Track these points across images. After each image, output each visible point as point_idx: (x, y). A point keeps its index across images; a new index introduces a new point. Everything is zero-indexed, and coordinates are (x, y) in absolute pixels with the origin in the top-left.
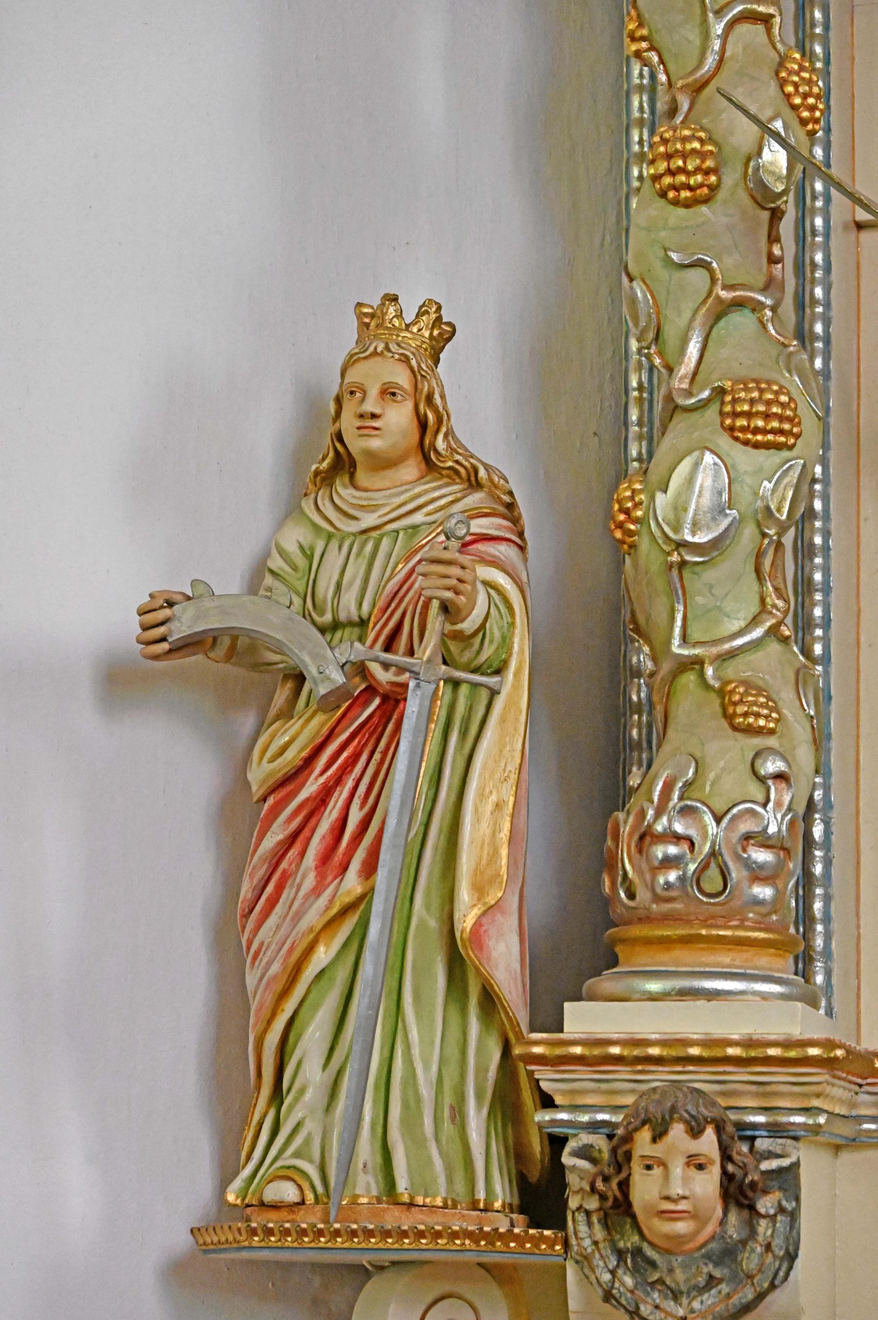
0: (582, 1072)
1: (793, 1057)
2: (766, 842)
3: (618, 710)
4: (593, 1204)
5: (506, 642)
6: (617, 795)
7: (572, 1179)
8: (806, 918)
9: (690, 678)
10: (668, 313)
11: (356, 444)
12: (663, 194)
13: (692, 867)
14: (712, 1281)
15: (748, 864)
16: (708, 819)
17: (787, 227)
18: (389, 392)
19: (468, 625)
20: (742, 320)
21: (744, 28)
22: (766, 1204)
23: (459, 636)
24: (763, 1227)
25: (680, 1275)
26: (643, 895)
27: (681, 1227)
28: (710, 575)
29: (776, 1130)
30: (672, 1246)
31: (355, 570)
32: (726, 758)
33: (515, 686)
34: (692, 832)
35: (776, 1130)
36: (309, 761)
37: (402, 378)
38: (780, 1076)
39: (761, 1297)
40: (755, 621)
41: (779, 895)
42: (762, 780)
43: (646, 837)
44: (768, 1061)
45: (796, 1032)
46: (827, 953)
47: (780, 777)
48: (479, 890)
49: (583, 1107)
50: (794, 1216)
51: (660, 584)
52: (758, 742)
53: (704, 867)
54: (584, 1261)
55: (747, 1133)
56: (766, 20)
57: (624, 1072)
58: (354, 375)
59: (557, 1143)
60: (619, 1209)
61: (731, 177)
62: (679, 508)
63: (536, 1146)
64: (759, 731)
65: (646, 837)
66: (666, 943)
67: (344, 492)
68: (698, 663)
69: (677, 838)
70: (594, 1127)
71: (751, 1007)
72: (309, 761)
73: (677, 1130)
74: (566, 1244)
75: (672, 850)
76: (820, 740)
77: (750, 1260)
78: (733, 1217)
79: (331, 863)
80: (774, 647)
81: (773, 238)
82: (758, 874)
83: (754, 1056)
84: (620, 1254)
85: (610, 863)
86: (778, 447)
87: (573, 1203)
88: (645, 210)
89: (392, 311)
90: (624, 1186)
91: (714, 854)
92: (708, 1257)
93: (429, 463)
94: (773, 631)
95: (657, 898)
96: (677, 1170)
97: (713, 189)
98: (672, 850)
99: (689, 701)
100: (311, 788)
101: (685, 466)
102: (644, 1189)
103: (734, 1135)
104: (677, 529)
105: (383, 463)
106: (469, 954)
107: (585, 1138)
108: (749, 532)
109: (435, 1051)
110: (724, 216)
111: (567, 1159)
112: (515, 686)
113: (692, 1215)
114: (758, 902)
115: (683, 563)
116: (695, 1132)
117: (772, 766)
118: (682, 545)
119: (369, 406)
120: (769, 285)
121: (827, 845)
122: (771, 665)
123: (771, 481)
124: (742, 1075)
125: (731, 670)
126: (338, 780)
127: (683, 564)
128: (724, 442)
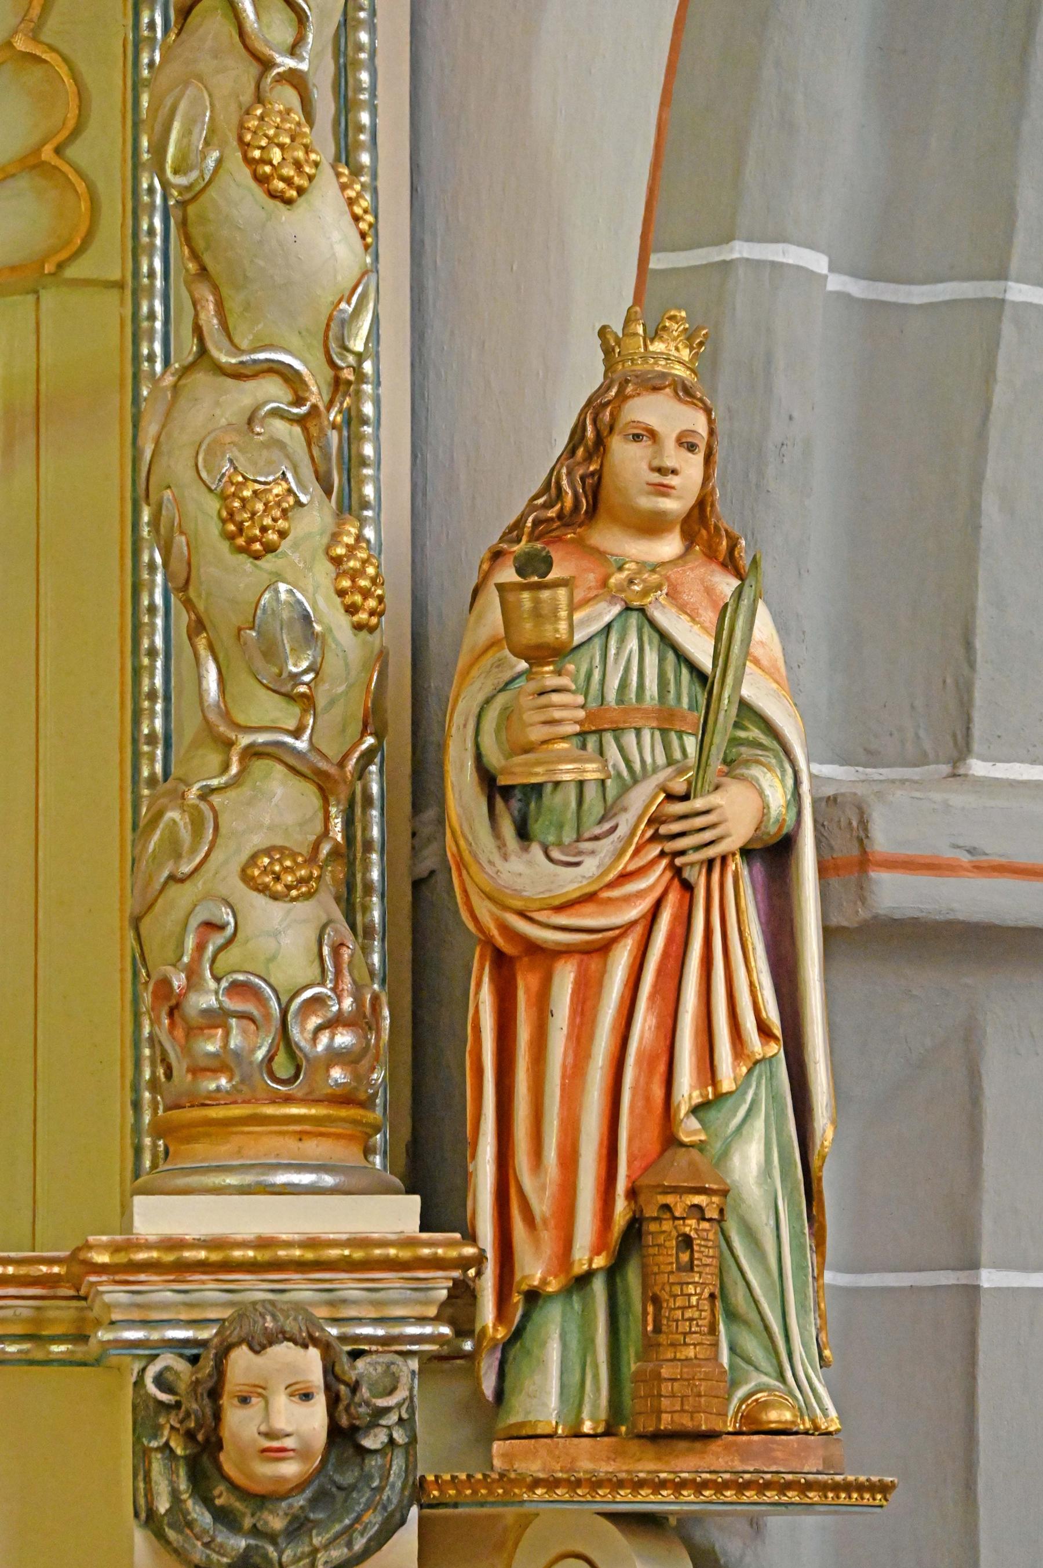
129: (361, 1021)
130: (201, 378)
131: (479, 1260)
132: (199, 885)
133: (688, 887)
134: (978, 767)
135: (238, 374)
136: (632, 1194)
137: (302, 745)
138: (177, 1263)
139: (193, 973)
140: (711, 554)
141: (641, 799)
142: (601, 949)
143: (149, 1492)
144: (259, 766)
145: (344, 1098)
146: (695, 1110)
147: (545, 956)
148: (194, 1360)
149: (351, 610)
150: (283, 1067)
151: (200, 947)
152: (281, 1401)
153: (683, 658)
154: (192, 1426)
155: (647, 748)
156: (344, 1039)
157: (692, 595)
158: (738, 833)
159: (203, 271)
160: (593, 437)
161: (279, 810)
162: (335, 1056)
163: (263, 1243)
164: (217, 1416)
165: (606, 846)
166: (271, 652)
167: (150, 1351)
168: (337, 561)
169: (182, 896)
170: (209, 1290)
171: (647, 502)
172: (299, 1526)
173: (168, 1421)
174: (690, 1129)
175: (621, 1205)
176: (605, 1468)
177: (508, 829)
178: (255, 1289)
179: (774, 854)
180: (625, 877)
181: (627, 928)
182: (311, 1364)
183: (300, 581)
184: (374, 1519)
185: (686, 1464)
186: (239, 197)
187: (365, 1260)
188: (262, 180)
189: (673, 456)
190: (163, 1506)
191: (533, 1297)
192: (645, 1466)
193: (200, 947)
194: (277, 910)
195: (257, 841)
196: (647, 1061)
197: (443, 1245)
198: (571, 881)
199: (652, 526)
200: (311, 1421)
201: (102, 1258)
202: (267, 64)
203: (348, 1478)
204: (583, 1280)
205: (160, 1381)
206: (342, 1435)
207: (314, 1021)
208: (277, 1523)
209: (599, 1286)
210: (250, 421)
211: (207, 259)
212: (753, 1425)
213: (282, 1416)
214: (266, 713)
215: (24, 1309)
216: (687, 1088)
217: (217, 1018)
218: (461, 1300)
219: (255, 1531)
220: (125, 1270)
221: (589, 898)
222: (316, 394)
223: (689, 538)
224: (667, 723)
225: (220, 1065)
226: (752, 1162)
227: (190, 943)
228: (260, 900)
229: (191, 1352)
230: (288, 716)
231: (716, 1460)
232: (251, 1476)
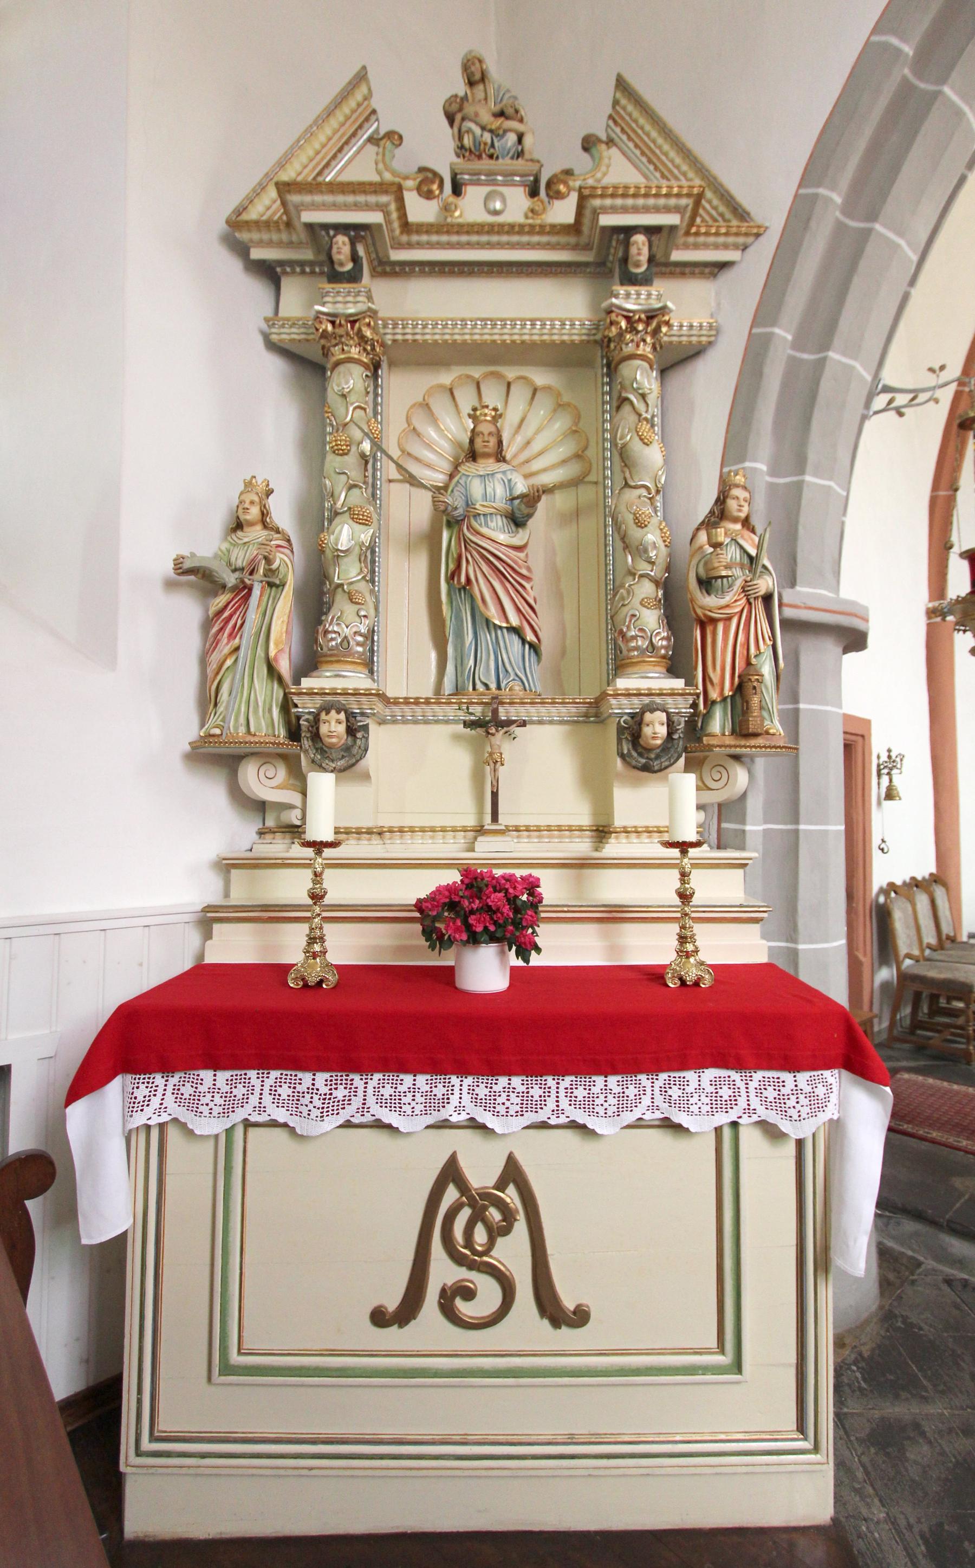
0: (306, 697)
1: (368, 694)
2: (361, 635)
3: (321, 603)
4: (308, 735)
5: (286, 576)
6: (320, 622)
7: (303, 728)
8: (373, 662)
9: (340, 590)
10: (335, 488)
11: (242, 517)
12: (334, 452)
13: (339, 640)
14: (343, 757)
15: (355, 640)
16: (344, 626)
17: (370, 466)
18: (252, 503)
19: (274, 566)
20: (356, 491)
21: (358, 411)
22: (359, 735)
23: (270, 570)
24: (358, 742)
25: (334, 755)
26: (325, 649)
27: (334, 740)
28: (345, 560)
29: (363, 714)
30: (331, 746)
31: (241, 554)
32: (349, 610)
33: (289, 590)
34: (340, 630)
35: (363, 714)
36: (226, 606)
37: (256, 499)
38: (364, 699)
39: (357, 761)
40: (359, 574)
41: (364, 651)
42: (360, 617)
43: (326, 632)
44: (361, 694)
45: (368, 686)
46: (378, 671)
47: (365, 616)
48: (276, 645)
49: (306, 706)
50: (367, 739)
51: (331, 562)
52: (358, 606)
53: (342, 641)
54: (306, 751)
55: (354, 715)
56: (365, 409)
57: (318, 697)
58: (243, 497)
59: (298, 718)
60: (316, 736)
61: (354, 449)
62: (337, 540)
63: (294, 720)
64: (359, 604)
65: (326, 632)
66: (331, 662)
67: (239, 533)
68: (341, 585)
69: (335, 632)
70: (310, 713)
71: (355, 679)
72: (226, 606)
73: (333, 712)
74: (301, 747)
75: (334, 636)
76: (377, 609)
77: (355, 750)
78: (349, 739)
79: (232, 636)
80: (364, 582)
81: (366, 470)
82: (358, 644)
83: (356, 693)
84: (317, 749)
85: (316, 640)
86: (367, 525)
87: (303, 735)
88: (330, 457)
89: (254, 481)
90: (318, 729)
91: (346, 637)
92: (342, 750)
93: (265, 526)
94: (364, 578)
95: (330, 650)
96: (333, 723)
97: (349, 451)
98: (334, 636)
99: (340, 599)
100: (226, 614)
101: (339, 528)
102: (324, 729)
103: (350, 716)
104: (337, 545)
105: (251, 524)
106: (274, 663)
107: (307, 716)
108: (357, 548)
109: (265, 694)
110: (351, 460)
111: (301, 722)
112: (289, 590)
113: (338, 737)
114: (358, 652)
115: (338, 556)
116: (338, 712)
117: (362, 613)
118: (338, 550)
119: (247, 505)
120: (365, 483)
121: (378, 641)
122: (363, 587)
123: (365, 535)
124: (353, 698)
125: (352, 587)
126: (235, 612)
127: (338, 556)
128: (351, 522)
129: (668, 639)
130: (627, 490)
131: (698, 695)
132: (630, 606)
133: (750, 604)
134: (798, 588)
135: (635, 487)
136: (739, 677)
137: (652, 574)
138: (628, 694)
139: (628, 627)
140: (748, 529)
141: (739, 583)
142: (729, 619)
143: (622, 750)
144: (643, 579)
145: (664, 657)
146: (755, 656)
147: (714, 621)
148: (632, 718)
149: (664, 541)
150: (650, 649)
151: (630, 621)
152: (657, 725)
153: (745, 551)
154: (632, 731)
155: (737, 572)
156: (665, 643)
157: (746, 536)
158: (762, 592)
159: (626, 465)
160: (721, 500)
161: (647, 589)
162: (662, 647)
163: (649, 689)
164: (640, 729)
165: (731, 594)
166: (646, 551)
167: (621, 715)
168: (661, 530)
169: (625, 610)
170: (635, 700)
171: (736, 514)
172: (658, 757)
173: (626, 732)
174: (754, 661)
175: (737, 679)
176: (733, 743)
177: (704, 591)
178: (647, 700)
179: (767, 599)
180: (736, 601)
181: (736, 613)
182: (663, 716)
183: (651, 537)
184: (676, 755)
185: (753, 742)
186: (636, 446)
187: (672, 694)
188: (642, 440)
189: (743, 503)
190: (625, 752)
191: (714, 702)
192: (743, 743)
193: (630, 621)
194: (649, 611)
195: (643, 596)
196: (742, 645)
197: (690, 690)
198: (723, 602)
199: (735, 520)
200: (663, 731)
201: (611, 693)
202: (640, 415)
203: (669, 745)
204: (724, 699)
205: (624, 722)
206: (670, 734)
207: (658, 638)
208: (653, 756)
209: (729, 700)
210: (640, 497)
211: (627, 462)
212: (767, 733)
213: (656, 728)
214: (644, 568)
215: (584, 710)
216: (753, 650)
217: (634, 638)
218: (694, 705)
219: (647, 758)
220: (616, 695)
221: (727, 606)
222: (653, 491)
223: (743, 526)
224: (742, 567)
225: (636, 648)
226: (767, 669)
227: (628, 620)
228: (644, 609)
229: (633, 716)
230: (649, 567)
231: (760, 741)
232: (649, 744)
